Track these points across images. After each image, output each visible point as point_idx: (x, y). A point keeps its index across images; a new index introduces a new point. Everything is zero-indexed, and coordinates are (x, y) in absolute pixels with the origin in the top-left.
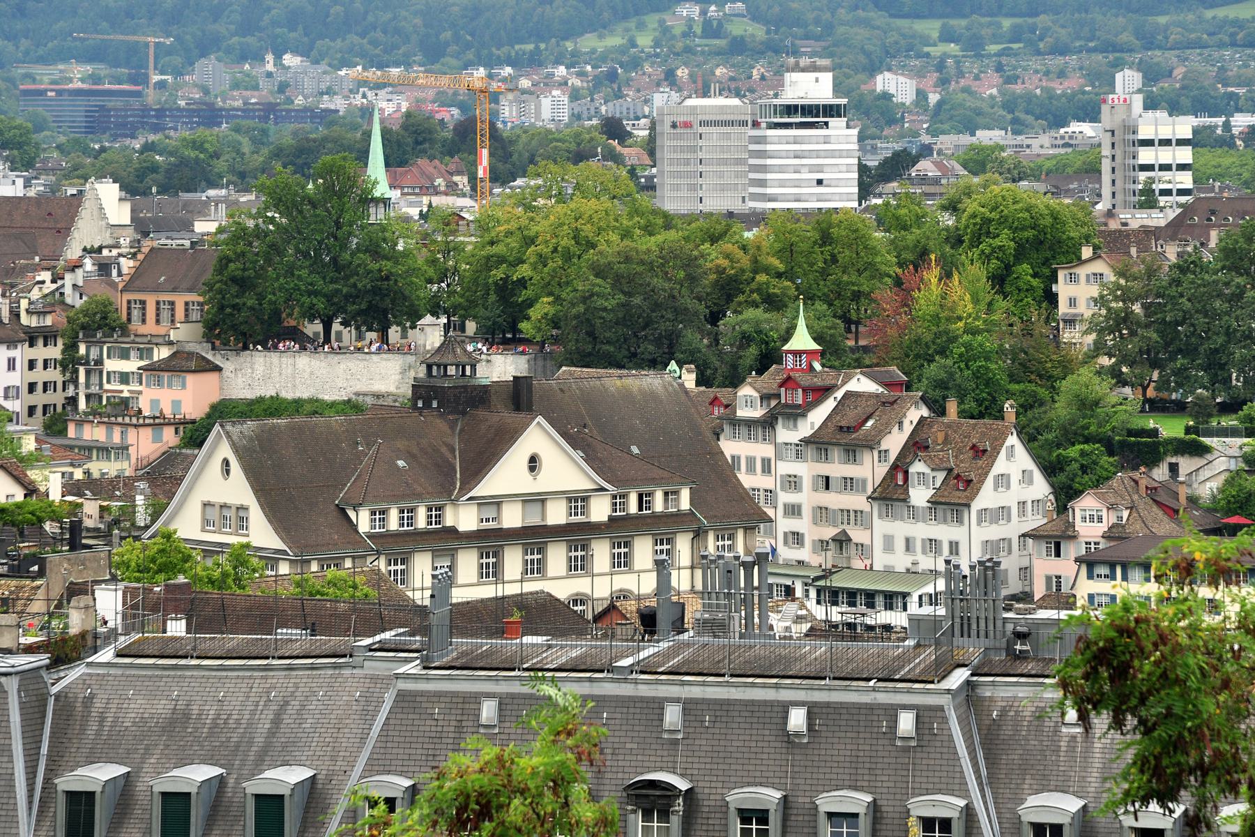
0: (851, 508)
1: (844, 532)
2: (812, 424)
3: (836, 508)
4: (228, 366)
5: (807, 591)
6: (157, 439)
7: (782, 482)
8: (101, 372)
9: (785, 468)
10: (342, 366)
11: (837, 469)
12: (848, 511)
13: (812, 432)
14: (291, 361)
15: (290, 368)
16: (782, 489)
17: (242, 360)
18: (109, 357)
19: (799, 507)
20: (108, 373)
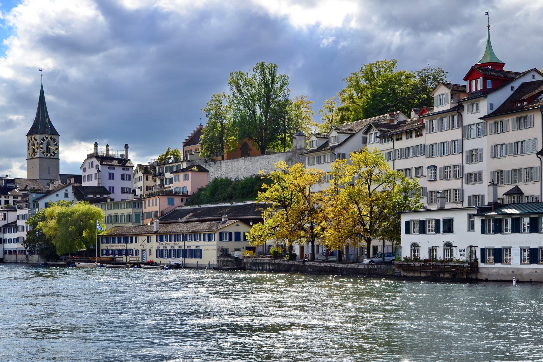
0: (523, 166)
1: (517, 188)
2: (491, 106)
3: (510, 169)
4: (211, 169)
5: (473, 222)
6: (171, 202)
7: (467, 157)
9: (469, 145)
10: (259, 163)
11: (511, 136)
12: (520, 170)
13: (491, 112)
14: (236, 163)
15: (236, 166)
16: (467, 161)
17: (216, 165)
19: (480, 174)
20: (166, 179)
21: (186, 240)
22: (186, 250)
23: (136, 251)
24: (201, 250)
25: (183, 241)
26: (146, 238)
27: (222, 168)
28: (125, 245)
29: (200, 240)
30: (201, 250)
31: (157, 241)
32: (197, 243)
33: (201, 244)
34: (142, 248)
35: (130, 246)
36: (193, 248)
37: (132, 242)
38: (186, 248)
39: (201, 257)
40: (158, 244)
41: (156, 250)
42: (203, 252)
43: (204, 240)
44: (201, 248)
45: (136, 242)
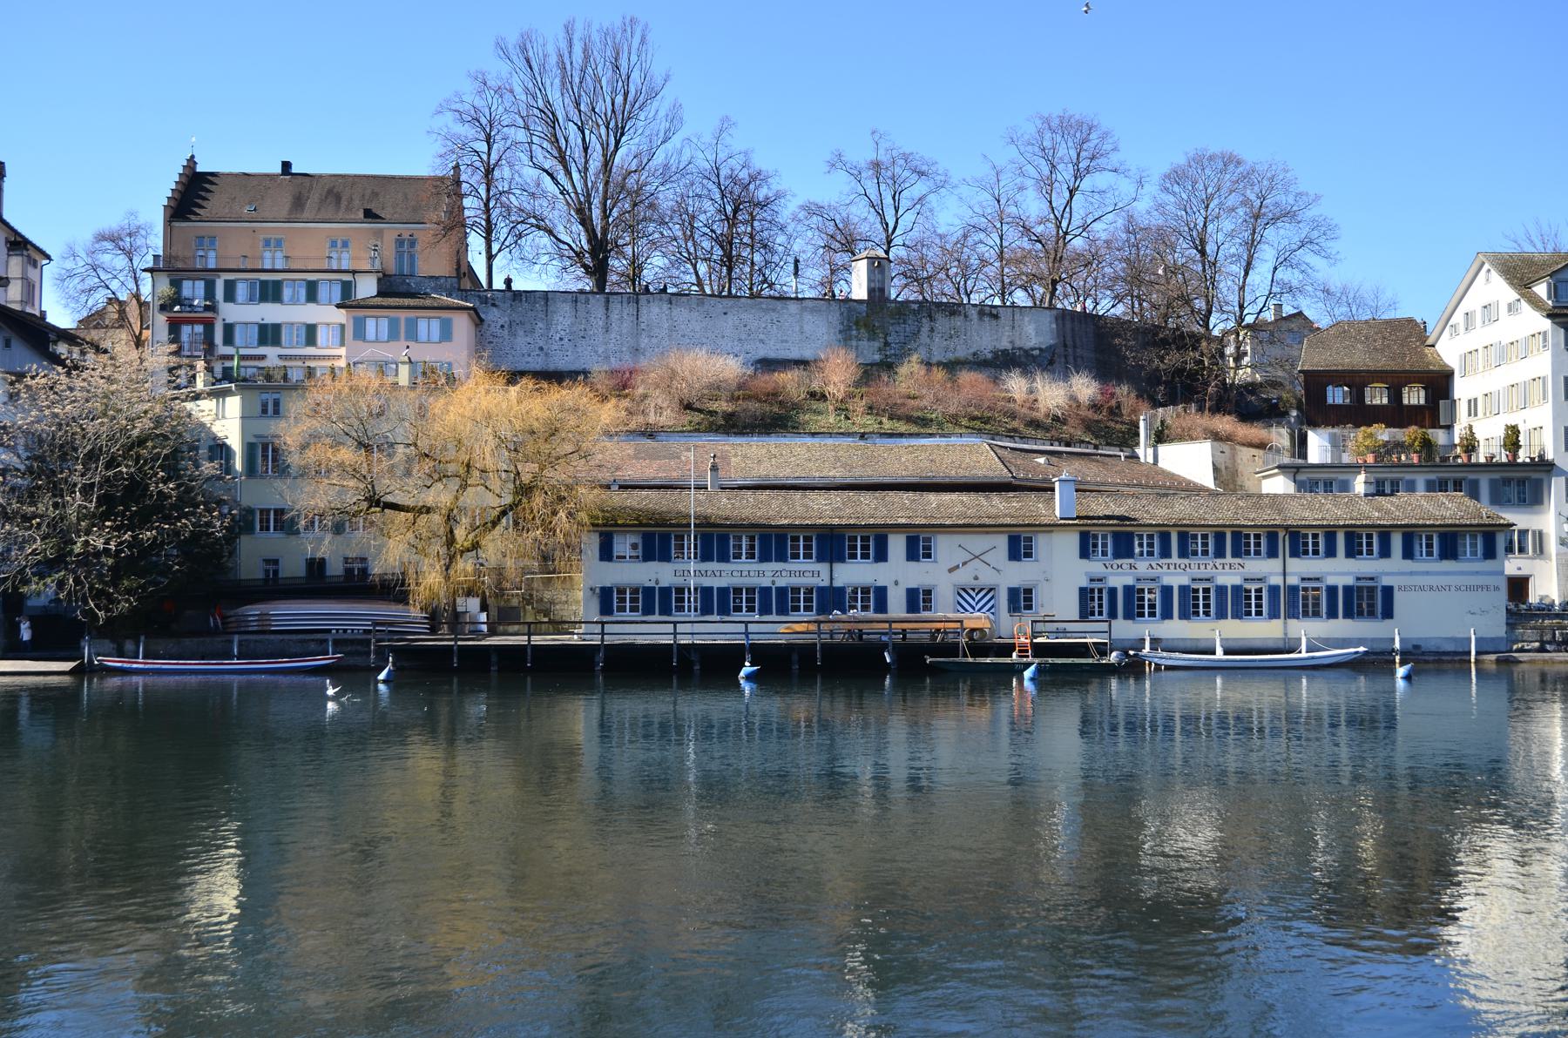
8: (209, 325)
18: (230, 296)
21: (1294, 554)
22: (1293, 590)
23: (912, 595)
24: (1388, 591)
25: (1272, 554)
26: (1002, 542)
27: (558, 318)
28: (823, 568)
29: (1385, 552)
30: (1388, 591)
31: (1084, 554)
32: (1366, 566)
33: (1389, 569)
34: (964, 577)
35: (853, 573)
36: (1341, 581)
37: (882, 556)
38: (1293, 580)
39: (1388, 613)
40: (1095, 566)
41: (1082, 591)
42: (1398, 597)
43: (1408, 554)
44: (1386, 581)
45: (912, 555)
